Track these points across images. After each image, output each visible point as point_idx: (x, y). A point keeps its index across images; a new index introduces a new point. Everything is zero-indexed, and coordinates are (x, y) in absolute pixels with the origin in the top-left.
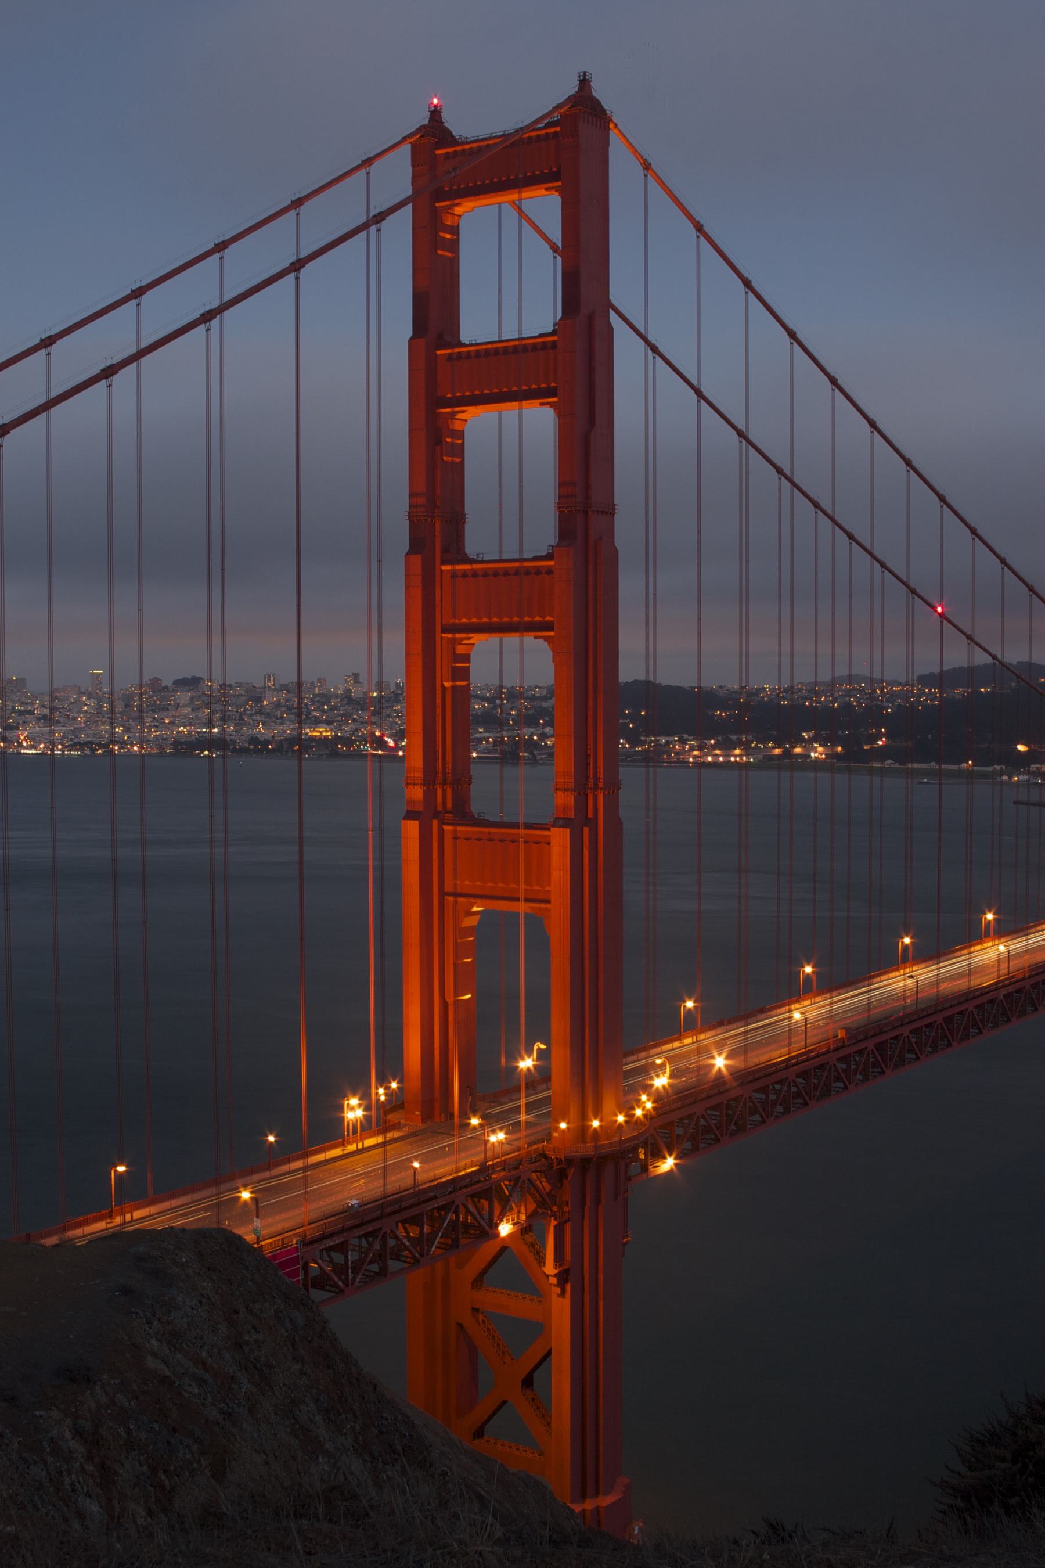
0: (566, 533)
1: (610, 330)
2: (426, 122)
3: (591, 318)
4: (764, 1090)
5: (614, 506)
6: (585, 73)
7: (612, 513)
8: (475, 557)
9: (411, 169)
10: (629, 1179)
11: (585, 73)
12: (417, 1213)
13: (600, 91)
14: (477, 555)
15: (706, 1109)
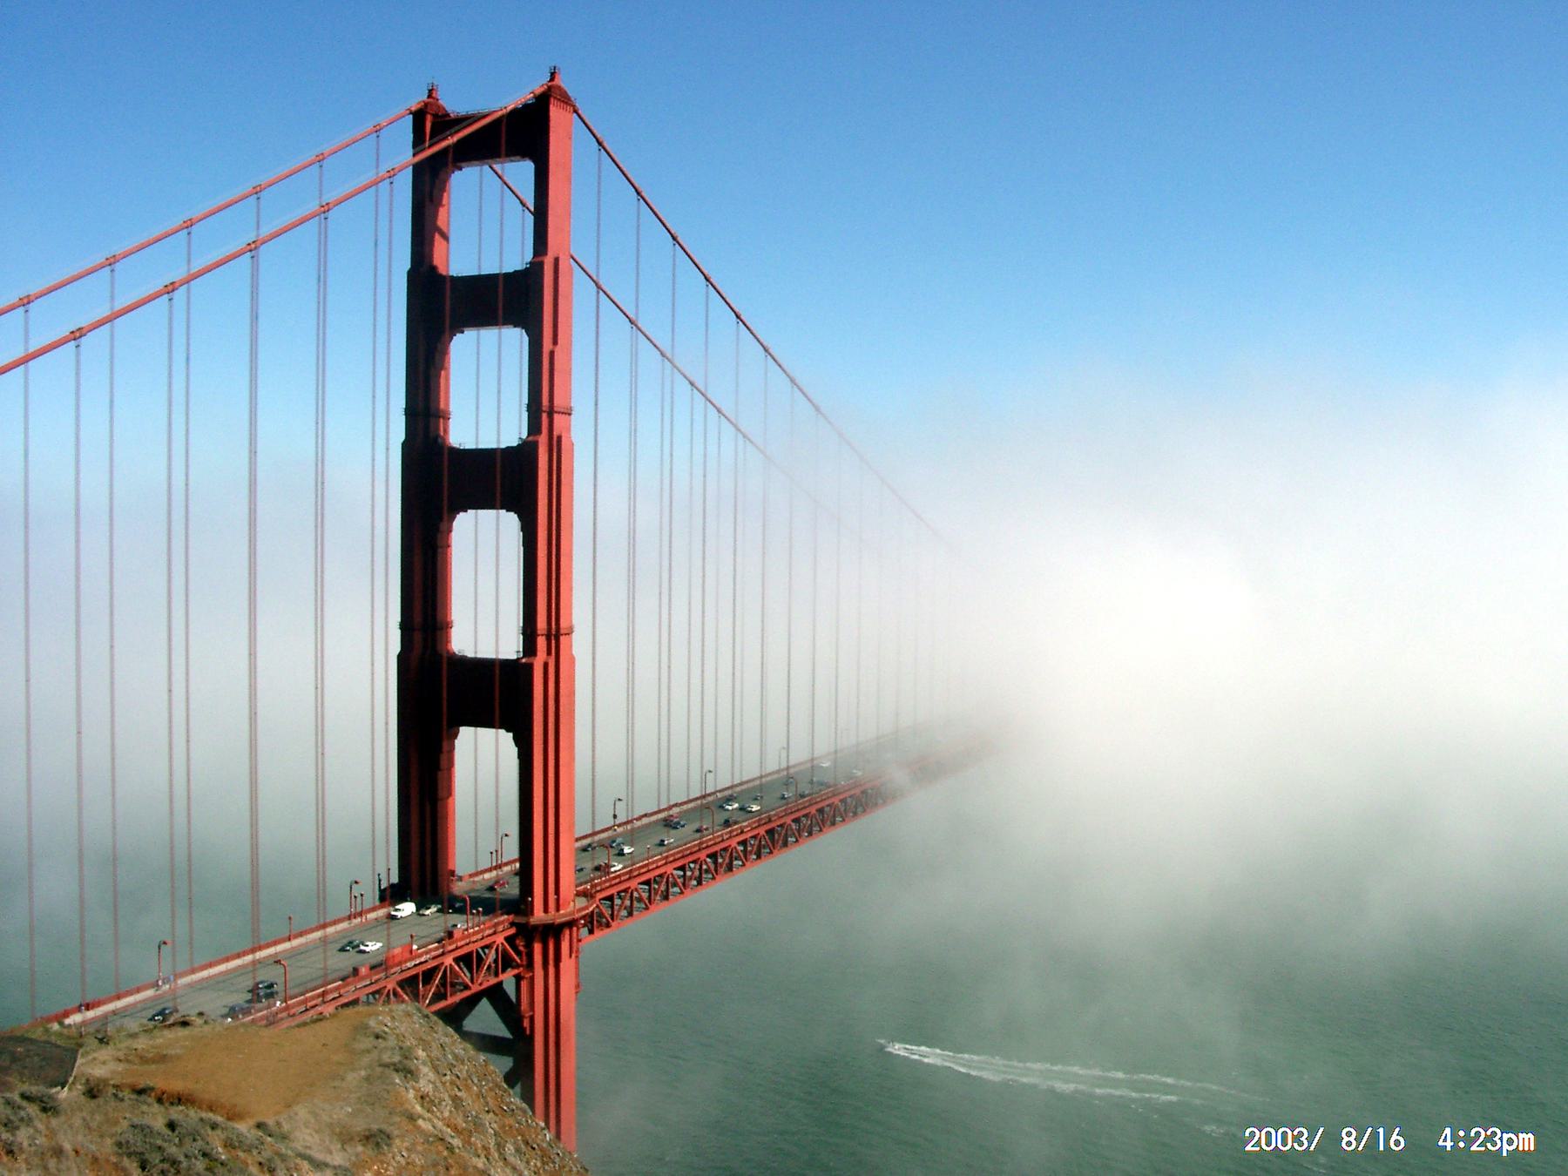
0: (534, 427)
1: (571, 269)
2: (425, 98)
3: (557, 260)
4: (682, 868)
5: (571, 409)
6: (555, 68)
7: (570, 414)
8: (458, 446)
9: (412, 135)
10: (579, 941)
11: (555, 68)
12: (414, 973)
13: (563, 82)
14: (460, 445)
15: (639, 884)
